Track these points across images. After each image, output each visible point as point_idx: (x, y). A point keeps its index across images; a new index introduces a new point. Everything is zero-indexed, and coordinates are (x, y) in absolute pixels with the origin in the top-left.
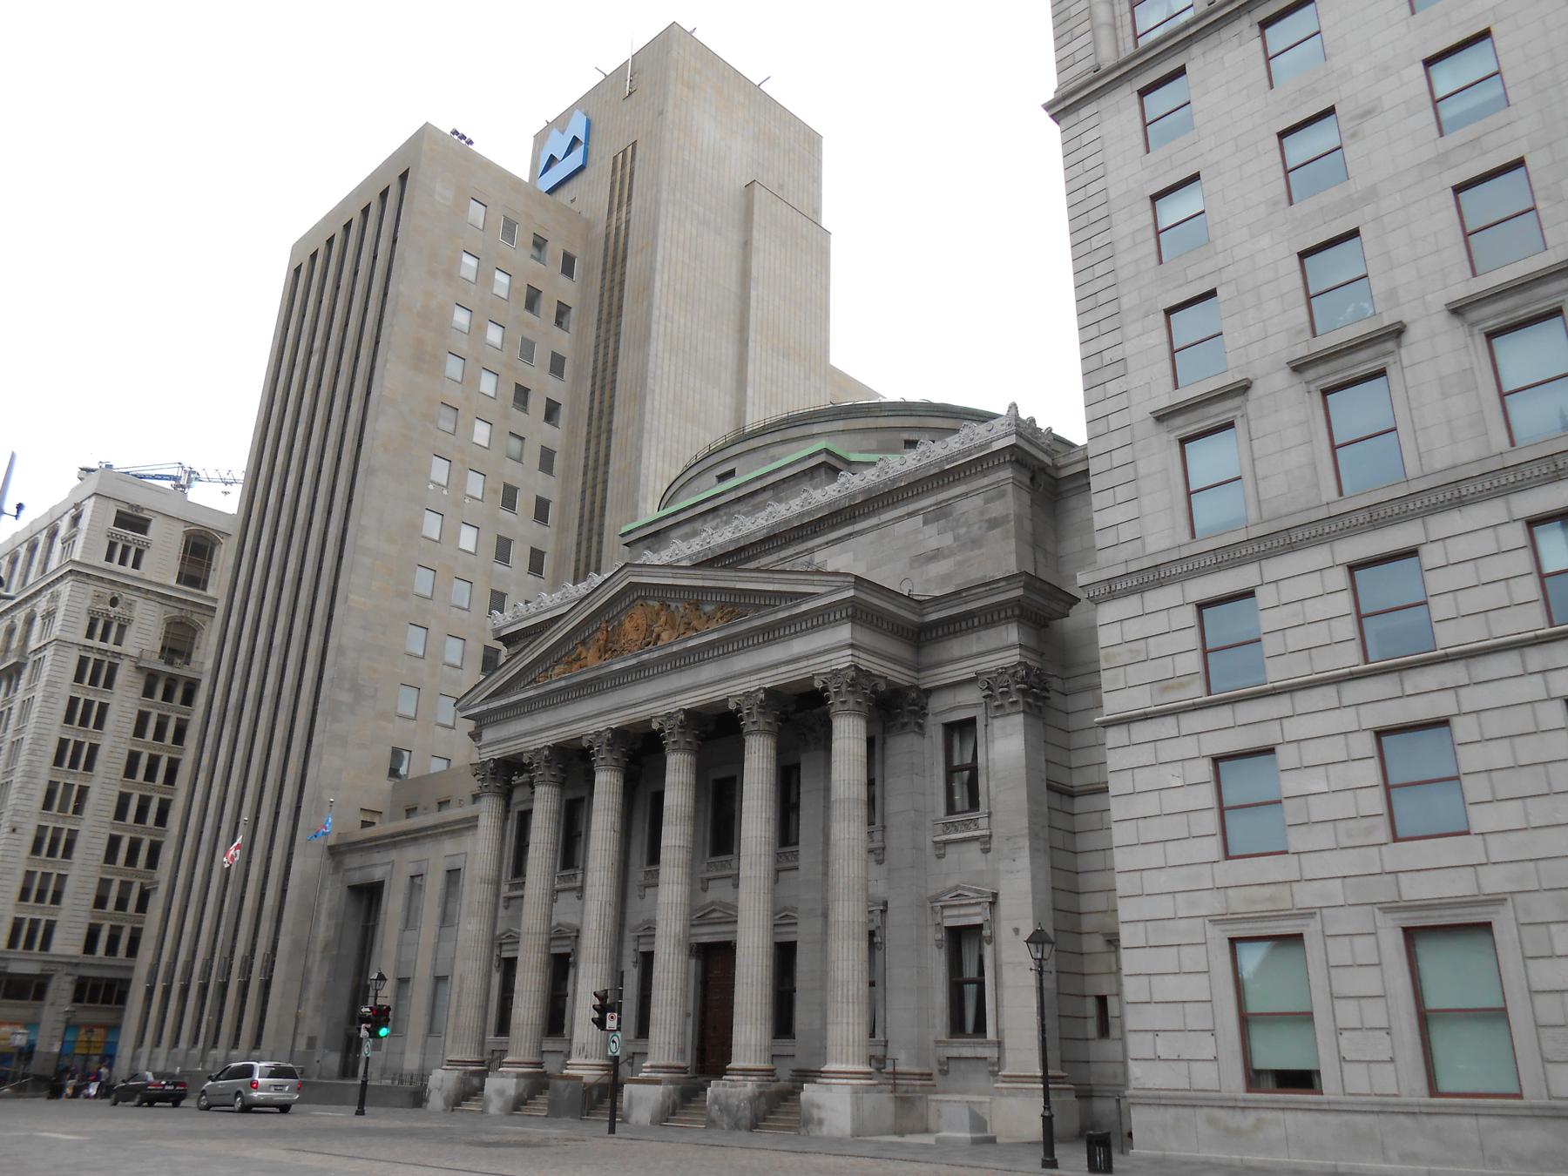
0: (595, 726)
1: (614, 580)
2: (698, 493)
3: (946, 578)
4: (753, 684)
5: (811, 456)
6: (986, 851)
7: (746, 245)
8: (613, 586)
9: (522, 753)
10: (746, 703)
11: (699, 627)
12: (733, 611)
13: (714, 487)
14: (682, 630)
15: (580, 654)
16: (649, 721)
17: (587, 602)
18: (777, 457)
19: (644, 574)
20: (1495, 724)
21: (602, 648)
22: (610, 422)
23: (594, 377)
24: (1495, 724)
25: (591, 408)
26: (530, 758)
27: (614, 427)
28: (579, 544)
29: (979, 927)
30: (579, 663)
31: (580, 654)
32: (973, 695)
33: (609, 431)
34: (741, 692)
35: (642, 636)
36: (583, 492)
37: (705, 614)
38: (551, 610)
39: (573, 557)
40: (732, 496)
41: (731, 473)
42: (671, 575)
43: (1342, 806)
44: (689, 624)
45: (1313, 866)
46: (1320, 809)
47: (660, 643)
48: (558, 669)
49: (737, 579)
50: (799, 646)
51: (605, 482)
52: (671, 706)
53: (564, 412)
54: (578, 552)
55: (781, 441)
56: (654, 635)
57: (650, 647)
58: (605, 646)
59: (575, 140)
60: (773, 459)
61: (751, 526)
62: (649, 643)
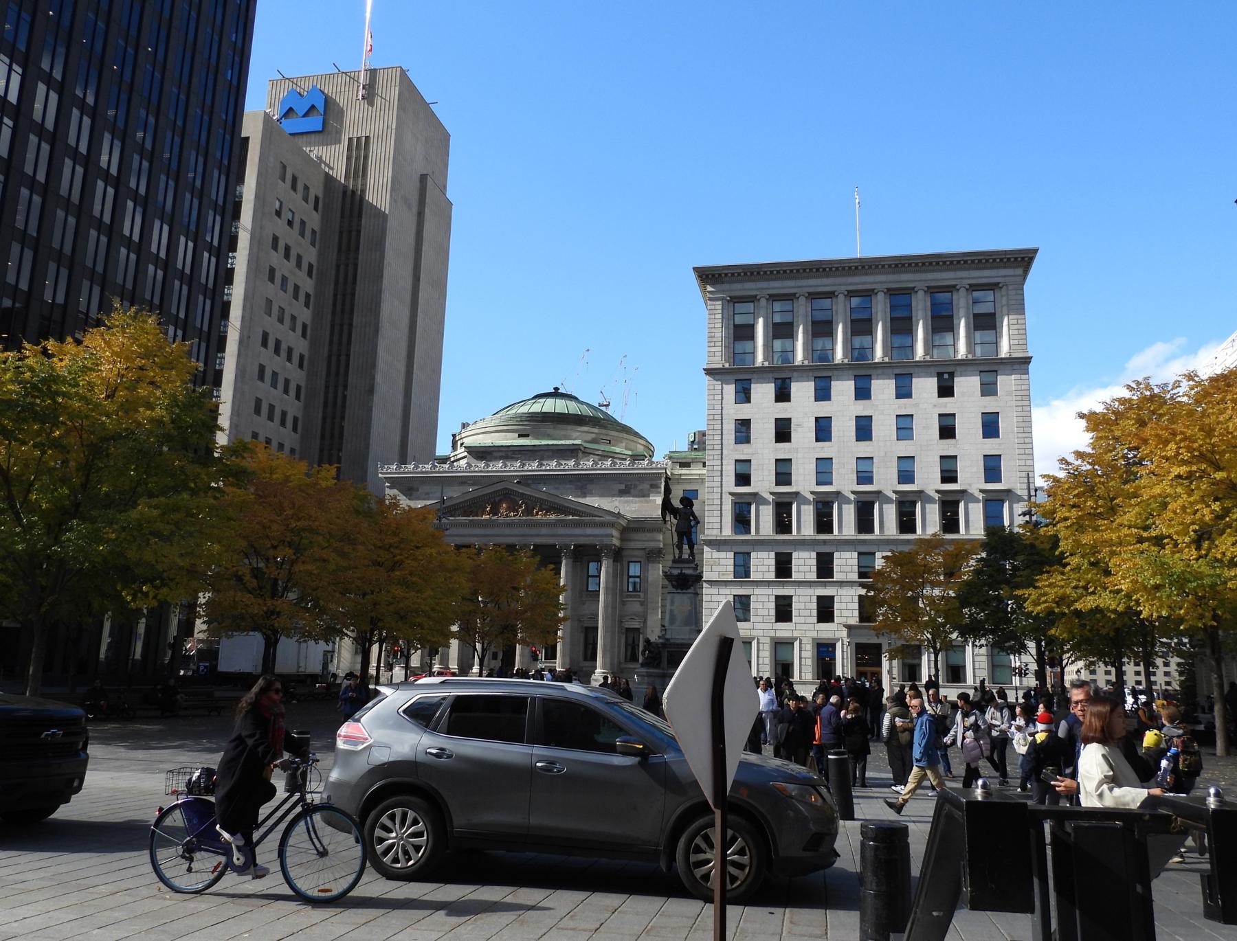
3: (633, 512)
6: (642, 605)
7: (420, 215)
20: (802, 599)
22: (352, 319)
23: (336, 283)
24: (802, 599)
25: (334, 304)
27: (354, 324)
28: (327, 387)
29: (639, 629)
32: (641, 553)
33: (351, 325)
36: (330, 357)
39: (322, 394)
43: (765, 612)
45: (757, 626)
46: (760, 612)
50: (589, 531)
51: (348, 356)
53: (312, 299)
54: (326, 393)
59: (313, 107)
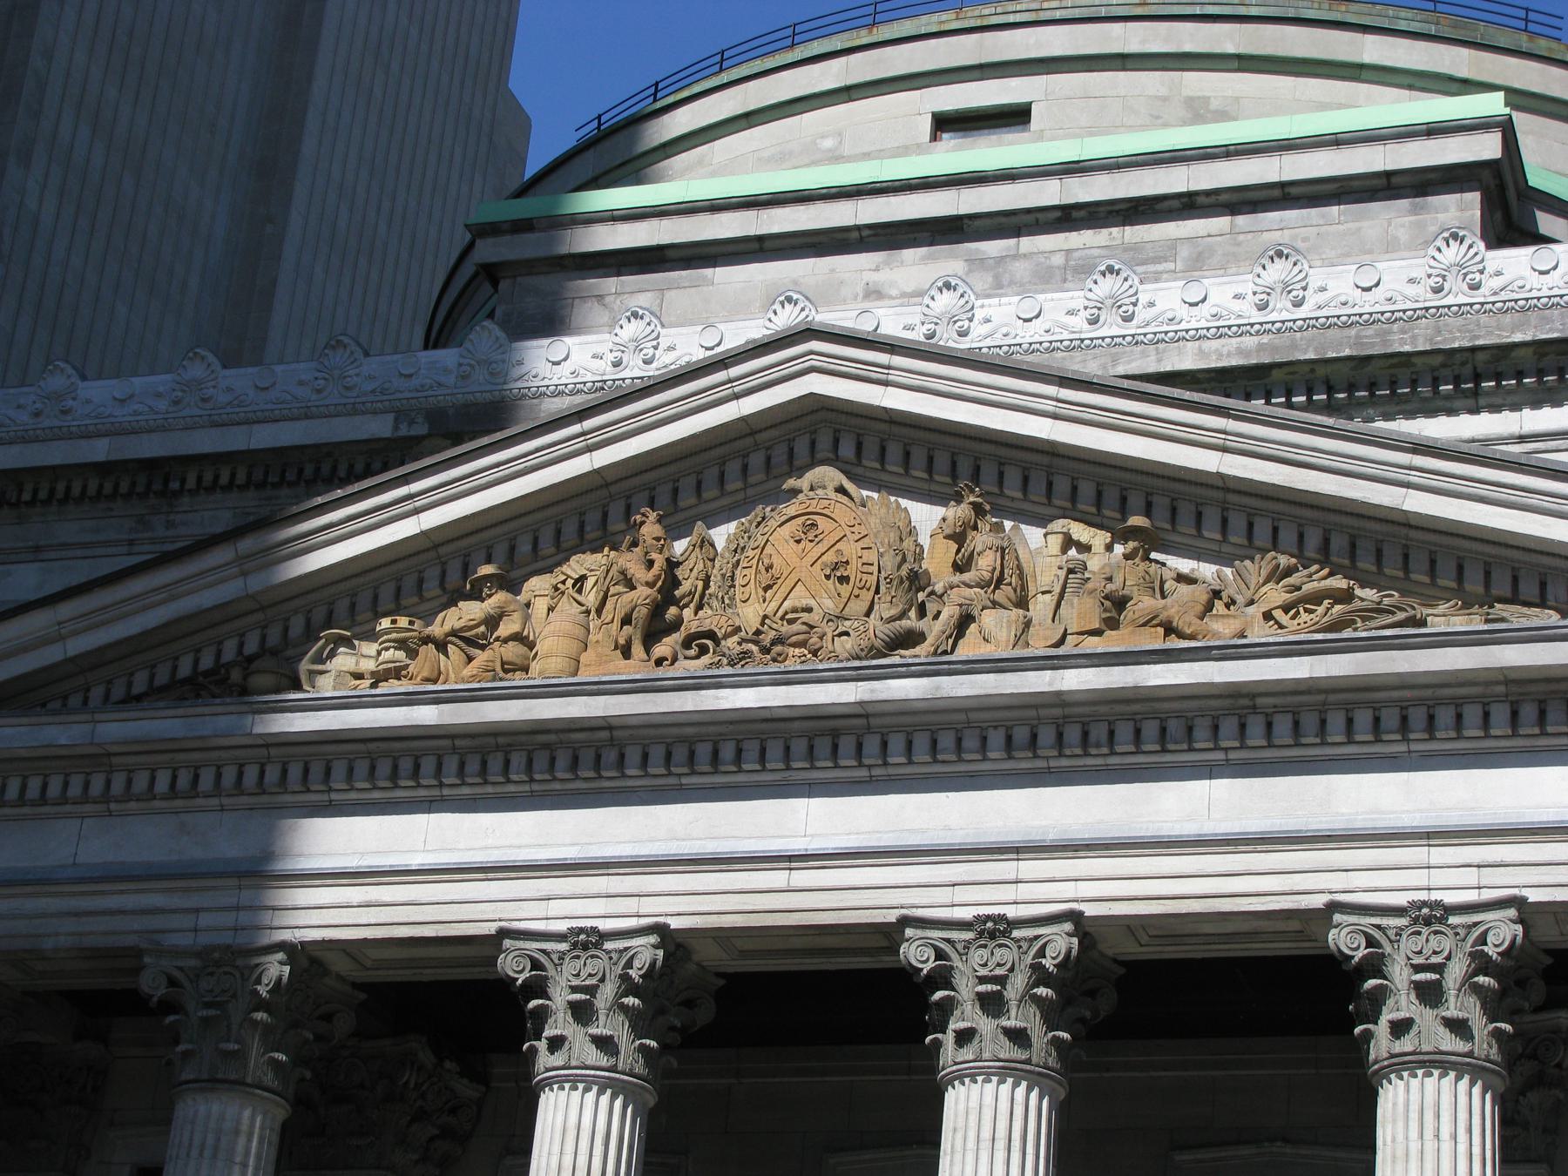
0: (556, 907)
1: (735, 371)
2: (835, 158)
4: (1439, 877)
5: (1433, 130)
8: (725, 392)
9: (137, 953)
10: (1408, 945)
11: (1187, 622)
12: (1346, 597)
13: (918, 149)
14: (1081, 611)
15: (492, 622)
16: (891, 934)
17: (575, 429)
18: (1214, 105)
19: (894, 376)
21: (642, 613)
26: (172, 982)
30: (482, 657)
31: (492, 622)
34: (1401, 899)
35: (858, 607)
37: (1181, 578)
38: (24, 439)
40: (1049, 193)
41: (1016, 116)
42: (1049, 406)
44: (1119, 603)
47: (969, 648)
48: (367, 656)
49: (1415, 477)
52: (1008, 893)
55: (1239, 57)
56: (949, 612)
57: (922, 651)
58: (657, 610)
60: (1198, 112)
61: (1183, 312)
62: (911, 639)
